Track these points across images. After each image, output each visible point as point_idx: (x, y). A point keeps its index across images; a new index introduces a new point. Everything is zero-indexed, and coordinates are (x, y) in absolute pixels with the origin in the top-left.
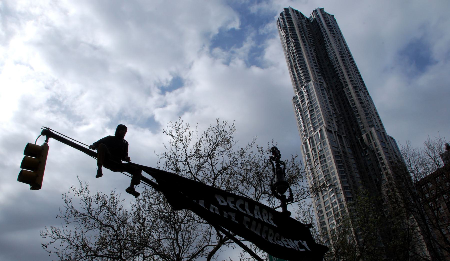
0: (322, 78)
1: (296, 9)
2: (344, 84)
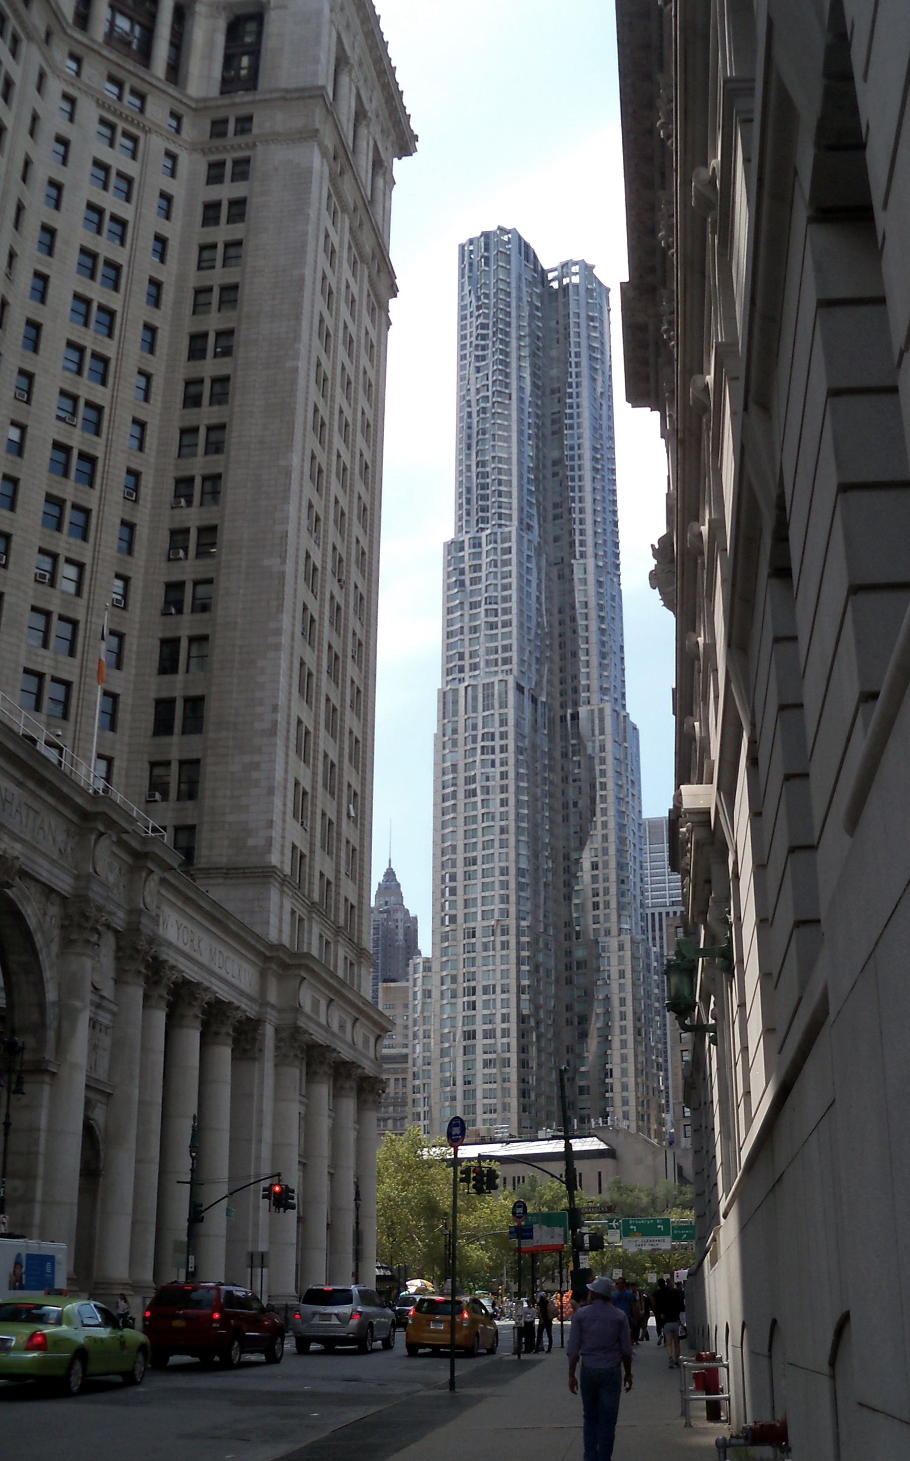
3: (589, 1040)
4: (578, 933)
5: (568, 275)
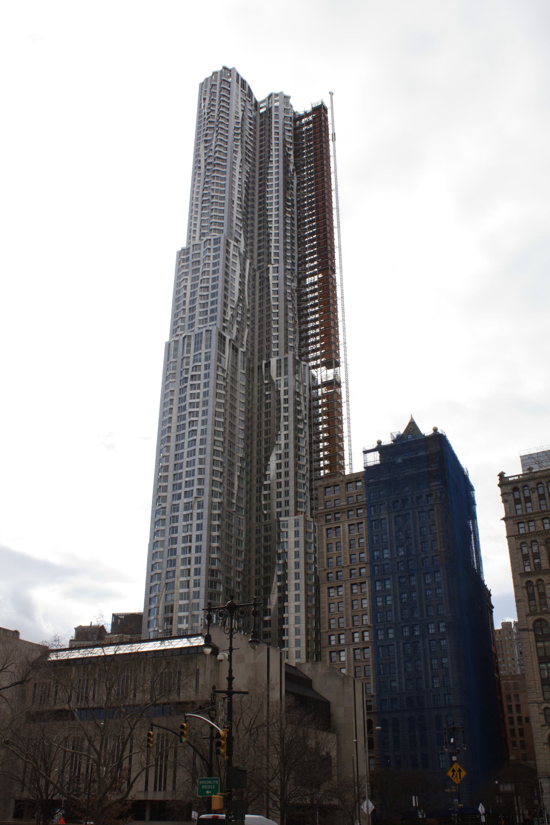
0: (242, 232)
1: (245, 78)
2: (273, 257)
3: (271, 596)
4: (265, 515)
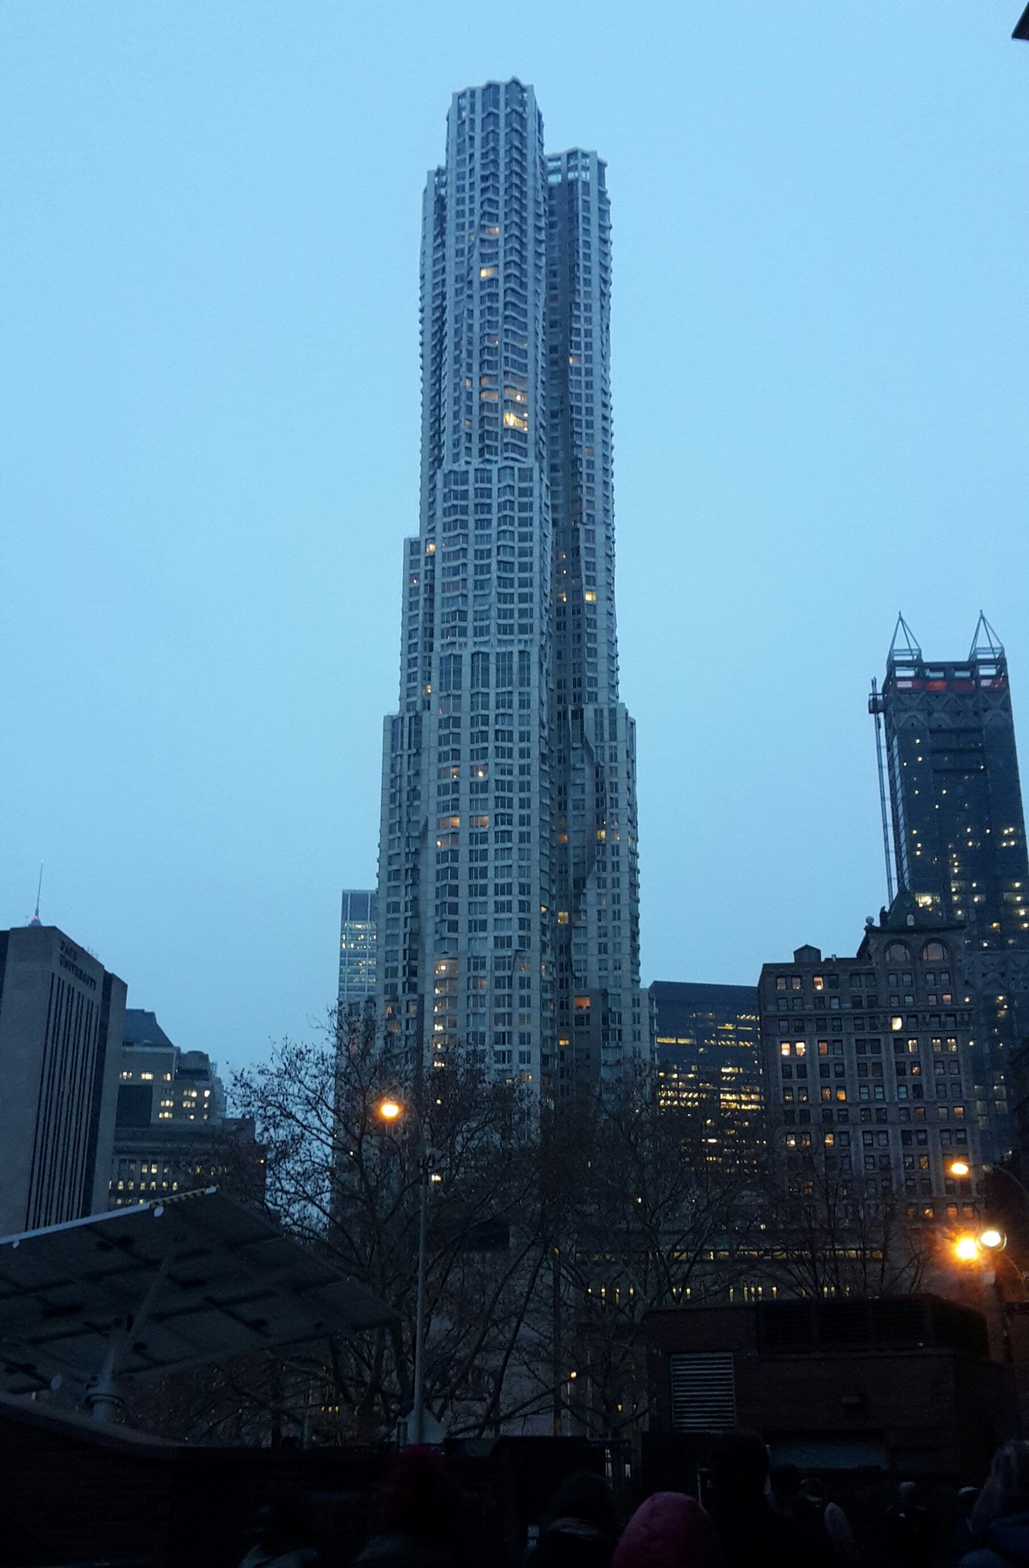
1: (541, 110)
5: (574, 168)
